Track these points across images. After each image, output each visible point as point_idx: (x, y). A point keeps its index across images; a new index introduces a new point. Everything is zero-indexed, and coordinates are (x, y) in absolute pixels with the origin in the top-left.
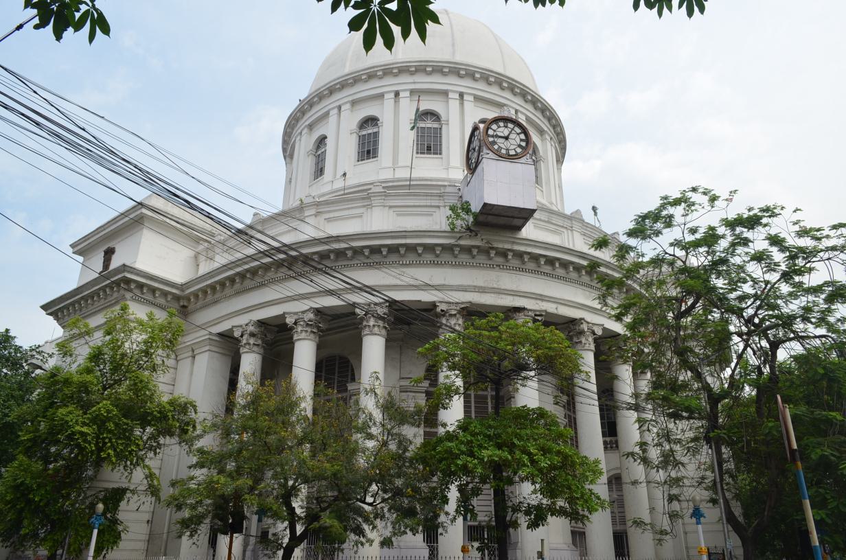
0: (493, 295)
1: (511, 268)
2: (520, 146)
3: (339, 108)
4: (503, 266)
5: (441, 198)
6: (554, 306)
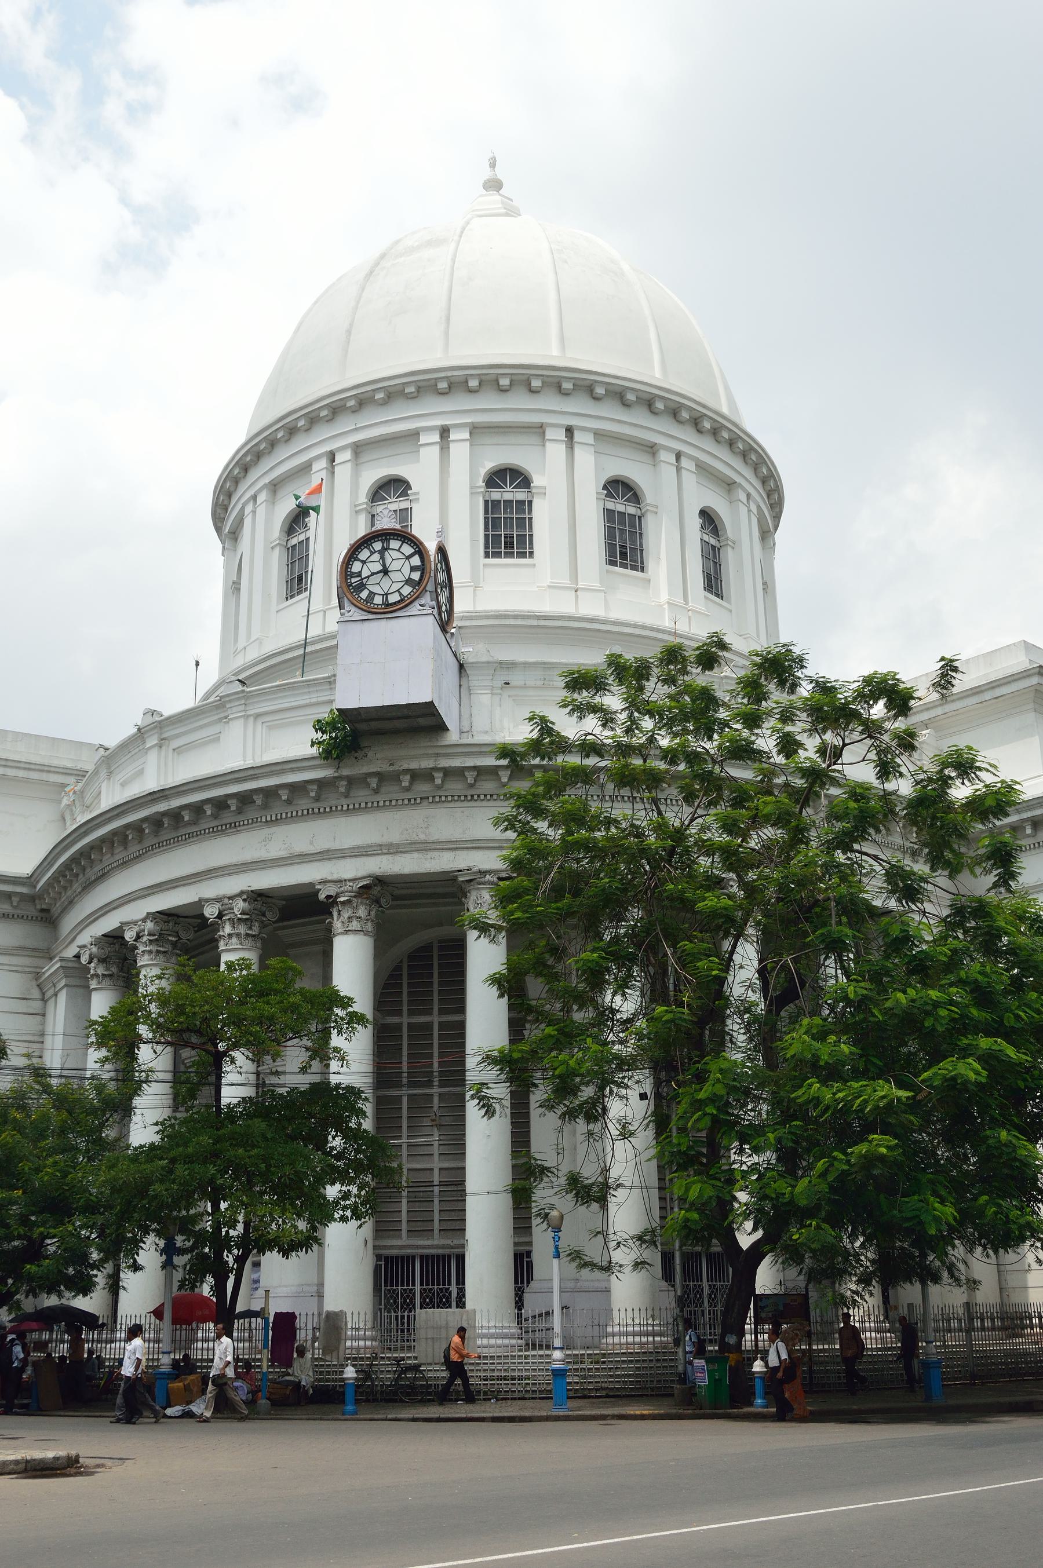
0: (415, 855)
2: (409, 581)
4: (434, 797)
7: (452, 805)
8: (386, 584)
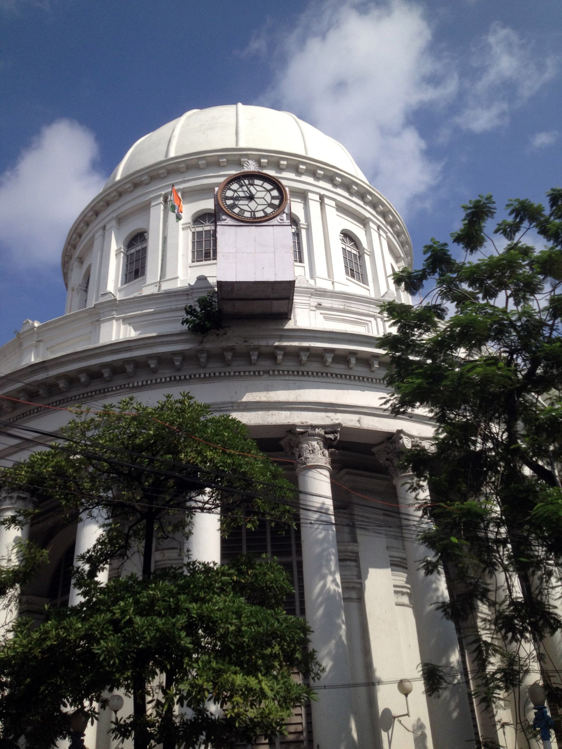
1: (286, 372)
2: (271, 205)
3: (104, 228)
5: (190, 297)
6: (355, 417)
7: (287, 378)
8: (253, 205)
